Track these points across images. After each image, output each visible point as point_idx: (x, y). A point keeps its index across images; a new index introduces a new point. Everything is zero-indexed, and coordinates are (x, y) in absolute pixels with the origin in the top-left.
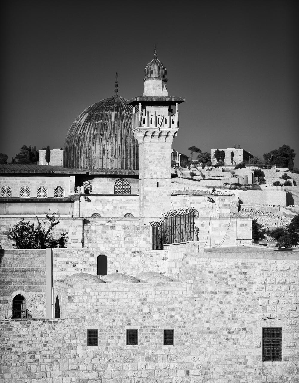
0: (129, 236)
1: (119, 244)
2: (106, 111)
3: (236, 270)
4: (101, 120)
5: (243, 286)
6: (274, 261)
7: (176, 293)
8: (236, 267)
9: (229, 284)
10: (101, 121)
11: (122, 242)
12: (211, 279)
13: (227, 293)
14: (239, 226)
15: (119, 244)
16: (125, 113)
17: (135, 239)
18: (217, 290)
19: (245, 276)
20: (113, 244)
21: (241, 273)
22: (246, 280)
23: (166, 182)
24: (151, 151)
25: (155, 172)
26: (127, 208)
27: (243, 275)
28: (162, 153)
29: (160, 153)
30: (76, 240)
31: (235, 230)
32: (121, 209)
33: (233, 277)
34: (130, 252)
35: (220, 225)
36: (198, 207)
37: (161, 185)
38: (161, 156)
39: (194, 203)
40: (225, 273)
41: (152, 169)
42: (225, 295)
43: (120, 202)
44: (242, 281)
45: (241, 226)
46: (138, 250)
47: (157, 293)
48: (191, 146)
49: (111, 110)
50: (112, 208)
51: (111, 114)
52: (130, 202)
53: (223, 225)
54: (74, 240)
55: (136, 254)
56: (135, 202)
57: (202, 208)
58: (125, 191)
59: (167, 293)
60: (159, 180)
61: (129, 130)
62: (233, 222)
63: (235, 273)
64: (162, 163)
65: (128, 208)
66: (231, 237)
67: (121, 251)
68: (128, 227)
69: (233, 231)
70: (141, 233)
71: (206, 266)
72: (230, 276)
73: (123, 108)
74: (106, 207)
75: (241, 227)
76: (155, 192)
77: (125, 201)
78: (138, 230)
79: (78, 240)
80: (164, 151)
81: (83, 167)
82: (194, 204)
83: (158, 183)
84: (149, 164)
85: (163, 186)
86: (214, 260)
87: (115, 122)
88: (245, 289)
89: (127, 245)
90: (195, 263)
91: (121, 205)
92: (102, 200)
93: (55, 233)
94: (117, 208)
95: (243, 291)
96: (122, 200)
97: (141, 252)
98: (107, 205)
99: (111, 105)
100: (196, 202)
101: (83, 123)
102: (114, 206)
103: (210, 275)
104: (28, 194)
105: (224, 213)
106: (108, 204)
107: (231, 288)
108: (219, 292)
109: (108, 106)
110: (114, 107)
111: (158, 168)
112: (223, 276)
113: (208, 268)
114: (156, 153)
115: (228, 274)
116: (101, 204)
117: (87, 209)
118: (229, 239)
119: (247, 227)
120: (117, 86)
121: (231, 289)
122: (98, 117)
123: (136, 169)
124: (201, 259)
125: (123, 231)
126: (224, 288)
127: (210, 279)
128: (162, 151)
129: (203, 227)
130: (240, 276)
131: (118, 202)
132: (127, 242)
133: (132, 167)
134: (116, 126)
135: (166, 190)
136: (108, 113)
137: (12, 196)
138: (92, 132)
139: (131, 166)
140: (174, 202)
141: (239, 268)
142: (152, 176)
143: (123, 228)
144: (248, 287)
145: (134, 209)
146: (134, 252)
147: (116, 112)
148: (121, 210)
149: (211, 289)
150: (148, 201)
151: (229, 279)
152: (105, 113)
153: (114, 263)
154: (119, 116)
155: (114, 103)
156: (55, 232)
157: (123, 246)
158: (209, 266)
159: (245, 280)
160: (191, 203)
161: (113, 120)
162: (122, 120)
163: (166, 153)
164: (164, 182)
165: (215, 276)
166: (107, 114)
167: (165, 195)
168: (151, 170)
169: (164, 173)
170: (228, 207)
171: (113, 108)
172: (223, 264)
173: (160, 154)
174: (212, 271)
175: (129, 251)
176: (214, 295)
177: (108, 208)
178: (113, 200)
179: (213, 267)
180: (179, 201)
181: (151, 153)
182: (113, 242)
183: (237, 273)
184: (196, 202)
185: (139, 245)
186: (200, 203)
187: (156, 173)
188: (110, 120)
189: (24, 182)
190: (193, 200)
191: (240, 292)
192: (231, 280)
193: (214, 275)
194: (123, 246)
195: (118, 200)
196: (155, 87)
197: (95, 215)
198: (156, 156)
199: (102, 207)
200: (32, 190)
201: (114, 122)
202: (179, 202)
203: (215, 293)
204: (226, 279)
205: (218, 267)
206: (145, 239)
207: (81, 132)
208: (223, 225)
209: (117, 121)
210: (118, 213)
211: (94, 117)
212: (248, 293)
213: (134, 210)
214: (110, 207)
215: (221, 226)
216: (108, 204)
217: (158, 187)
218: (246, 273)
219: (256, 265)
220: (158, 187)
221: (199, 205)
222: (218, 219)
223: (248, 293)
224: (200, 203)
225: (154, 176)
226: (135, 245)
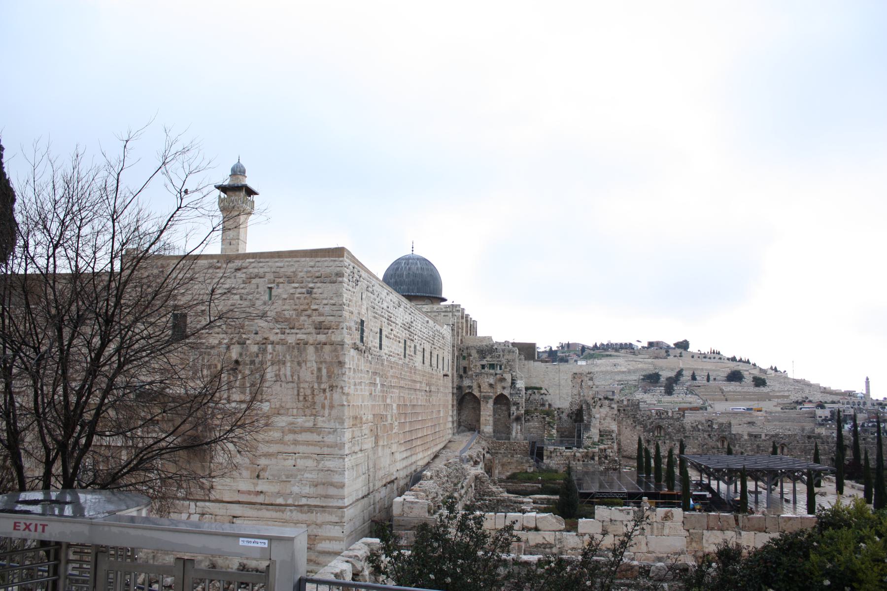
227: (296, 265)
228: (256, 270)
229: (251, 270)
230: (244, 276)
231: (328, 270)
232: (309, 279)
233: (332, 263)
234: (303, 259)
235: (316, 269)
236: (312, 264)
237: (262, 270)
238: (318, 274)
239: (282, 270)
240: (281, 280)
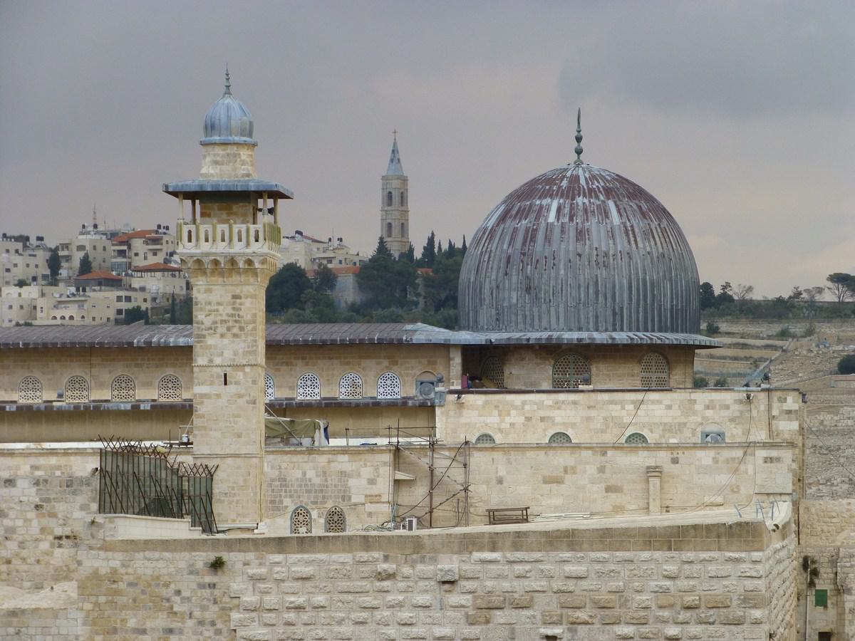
0: (48, 500)
1: (26, 520)
2: (540, 198)
3: (192, 577)
4: (526, 219)
5: (208, 615)
6: (279, 558)
7: (54, 631)
8: (191, 573)
9: (176, 609)
10: (524, 222)
11: (32, 515)
12: (134, 601)
13: (171, 631)
14: (760, 461)
15: (26, 520)
16: (580, 204)
17: (61, 508)
18: (149, 625)
19: (212, 593)
20: (11, 519)
21: (202, 586)
22: (215, 602)
23: (245, 374)
24: (210, 304)
25: (219, 351)
26: (556, 421)
27: (208, 591)
28: (234, 309)
29: (230, 307)
30: (376, 496)
31: (751, 472)
32: (543, 423)
33: (185, 594)
34: (51, 538)
35: (716, 460)
36: (724, 417)
37: (233, 380)
38: (232, 315)
39: (714, 408)
40: (167, 585)
41: (211, 345)
42: (167, 636)
43: (540, 405)
44: (205, 602)
45: (766, 462)
46: (69, 533)
47: (11, 630)
48: (844, 271)
49: (551, 197)
50: (522, 420)
51: (549, 207)
52: (564, 406)
53: (721, 459)
54: (372, 496)
55: (64, 542)
56: (573, 406)
57: (732, 420)
58: (578, 381)
59: (32, 631)
60: (228, 370)
61: (587, 241)
63: (188, 585)
64: (235, 330)
65: (558, 419)
66: (742, 488)
67: (31, 536)
68: (46, 481)
69: (747, 473)
70: (74, 493)
71: (123, 571)
72: (178, 592)
73: (579, 191)
74: (508, 420)
75: (766, 465)
76: (218, 396)
77: (551, 404)
78: (67, 486)
79: (380, 496)
80: (241, 304)
81: (486, 327)
82: (713, 409)
83: (225, 375)
84: (204, 332)
85: (237, 383)
86: (140, 555)
87: (556, 224)
88: (213, 623)
89: (46, 521)
90: (97, 564)
91: (542, 413)
92: (499, 402)
93: (329, 482)
94: (534, 420)
95: (209, 627)
96: (543, 401)
97: (75, 538)
98: (509, 415)
99: (556, 184)
100: (717, 407)
101: (489, 228)
102: (527, 415)
103: (131, 590)
104: (358, 390)
105: (783, 431)
106: (513, 412)
107: (179, 620)
108: (153, 629)
109: (547, 187)
110: (560, 187)
111: (226, 341)
112: (164, 592)
113: (127, 574)
114: (221, 308)
115: (172, 586)
116: (496, 412)
117: (466, 424)
118: (738, 492)
119: (779, 465)
120: (579, 139)
121: (179, 622)
122: (522, 213)
123: (641, 329)
124: (110, 554)
125: (34, 490)
126: (161, 621)
127: (131, 601)
128: (234, 303)
129: (677, 465)
130: (199, 592)
131: (535, 407)
132: (43, 515)
133: (591, 325)
134: (557, 231)
135: (243, 392)
136: (545, 202)
137: (403, 396)
138: (505, 247)
139: (588, 323)
140: (666, 405)
141: (197, 573)
142: (211, 361)
143: (34, 484)
144: (220, 617)
145: (571, 423)
146: (60, 538)
147: (561, 201)
148: (542, 425)
149: (132, 623)
150: (203, 416)
151: (177, 599)
152: (538, 202)
153: (14, 561)
154: (567, 210)
155: (562, 180)
156: (329, 479)
157: (35, 523)
158: (130, 570)
159: (212, 602)
160: (708, 407)
161: (552, 218)
162: (571, 219)
163: (243, 307)
164: (240, 374)
165: (143, 592)
166: (541, 207)
167: (242, 402)
168: (210, 347)
169: (241, 351)
170: (793, 416)
171: (558, 191)
172: (161, 564)
173: (231, 311)
174: (136, 581)
175: (49, 534)
176: (141, 637)
177: (512, 421)
178: (524, 403)
179: (139, 571)
180: (678, 402)
181: (208, 307)
182: (12, 514)
183: (194, 586)
185: (70, 522)
186: (727, 407)
187: (222, 354)
188: (545, 220)
190: (712, 401)
191: (201, 628)
192: (179, 601)
193: (140, 591)
194: (35, 523)
195: (535, 403)
196: (218, 159)
197: (563, 437)
198: (221, 315)
199: (497, 419)
200: (365, 381)
201: (552, 224)
202: (677, 406)
203: (144, 632)
204: (168, 600)
205: (149, 572)
206: (84, 507)
207: (484, 250)
208: (721, 459)
209: (560, 221)
210: (534, 433)
211: (514, 212)
212: (218, 632)
213: (573, 425)
214: (516, 418)
215: (717, 462)
216: (513, 412)
217: (226, 384)
218: (214, 585)
219: (239, 565)
220: (226, 384)
221: (726, 413)
223: (218, 632)
224: (727, 407)
225: (218, 361)
226: (61, 522)
227: (625, 571)
228: (506, 585)
229: (489, 584)
230: (466, 600)
231: (718, 588)
232: (666, 613)
233: (729, 568)
234: (645, 555)
235: (683, 584)
236: (671, 568)
237: (520, 586)
238: (689, 599)
239: (584, 584)
240: (582, 615)
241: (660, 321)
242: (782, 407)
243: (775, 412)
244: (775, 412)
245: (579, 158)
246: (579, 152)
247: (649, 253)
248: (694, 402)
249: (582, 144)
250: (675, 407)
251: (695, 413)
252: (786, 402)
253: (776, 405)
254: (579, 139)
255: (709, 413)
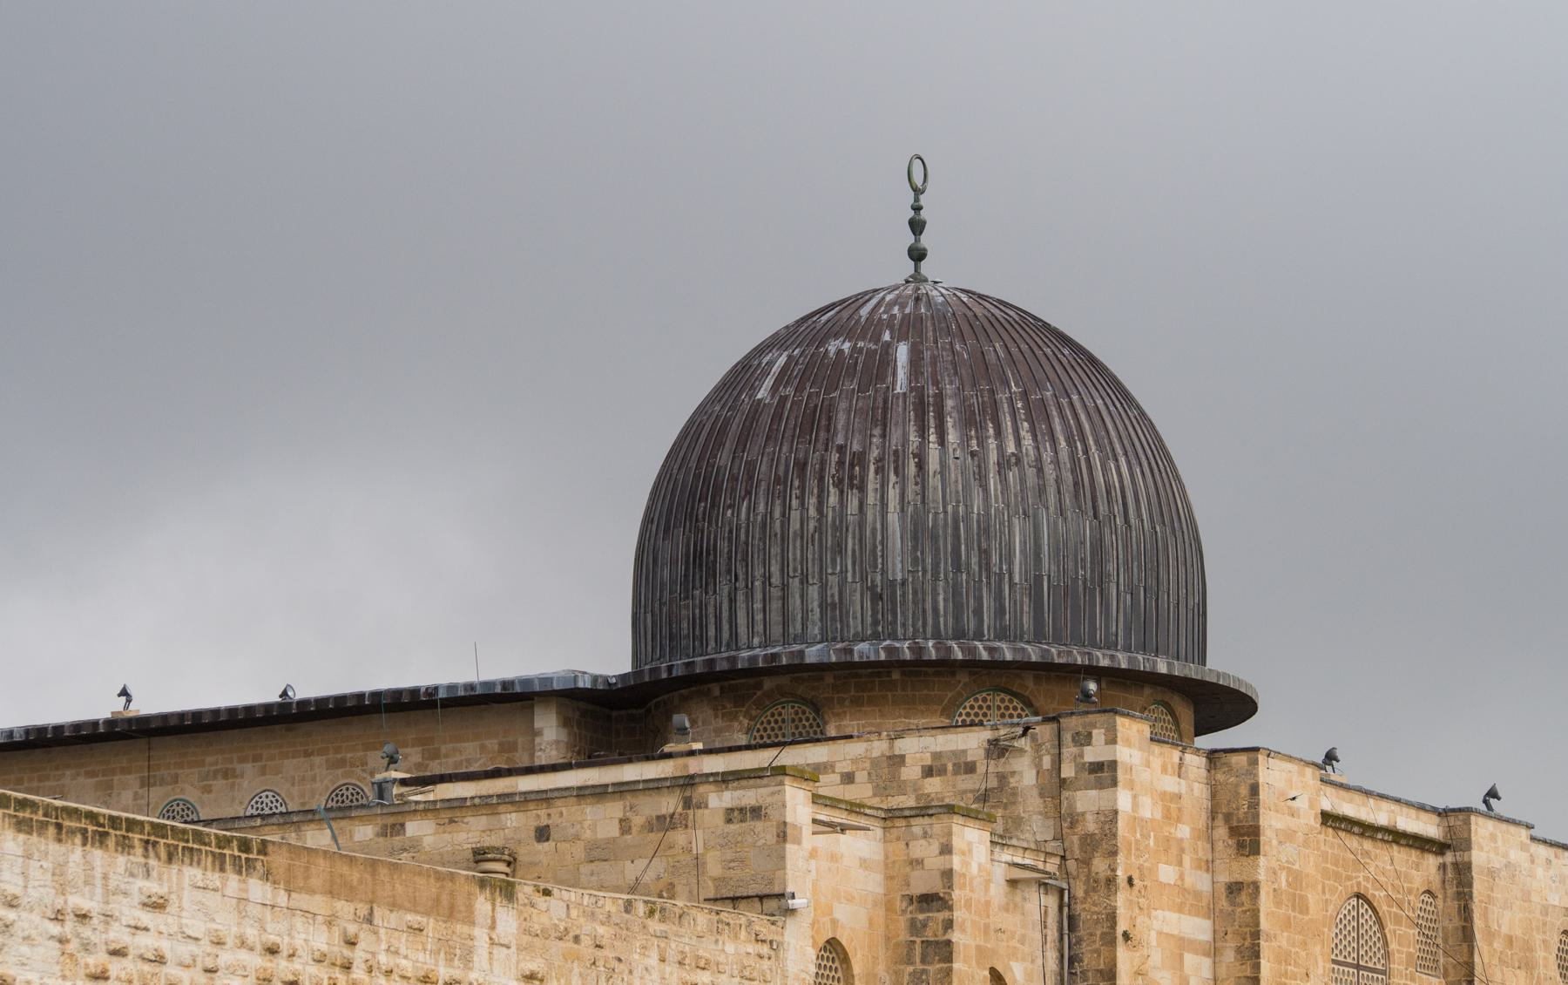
14: (719, 820)
36: (965, 792)
39: (942, 771)
45: (729, 821)
53: (637, 821)
62: (687, 803)
75: (732, 827)
100: (950, 767)
119: (759, 825)
120: (917, 226)
160: (929, 772)
180: (868, 765)
184: (950, 767)
186: (970, 768)
189: (342, 763)
190: (937, 756)
208: (637, 821)
222: (610, 789)
224: (970, 768)
241: (1000, 611)
242: (1081, 755)
243: (1068, 771)
244: (1068, 771)
245: (917, 269)
246: (917, 255)
247: (973, 454)
248: (898, 761)
249: (926, 240)
250: (861, 776)
251: (902, 789)
252: (1089, 744)
253: (1069, 750)
254: (917, 226)
255: (933, 786)
